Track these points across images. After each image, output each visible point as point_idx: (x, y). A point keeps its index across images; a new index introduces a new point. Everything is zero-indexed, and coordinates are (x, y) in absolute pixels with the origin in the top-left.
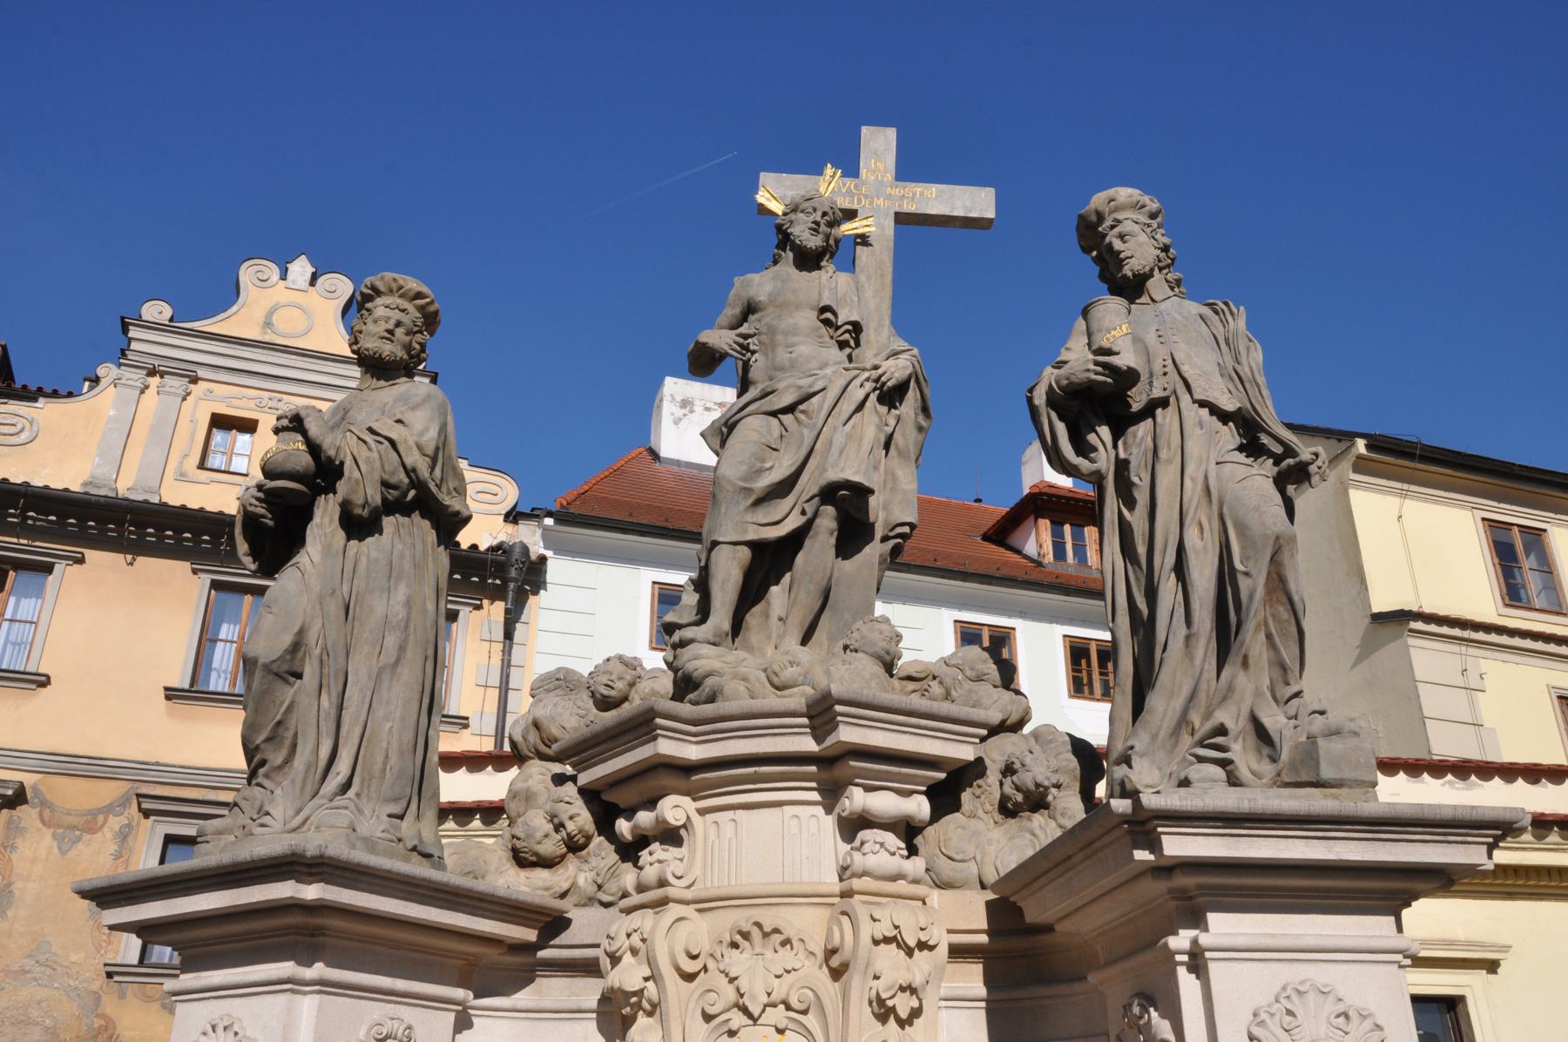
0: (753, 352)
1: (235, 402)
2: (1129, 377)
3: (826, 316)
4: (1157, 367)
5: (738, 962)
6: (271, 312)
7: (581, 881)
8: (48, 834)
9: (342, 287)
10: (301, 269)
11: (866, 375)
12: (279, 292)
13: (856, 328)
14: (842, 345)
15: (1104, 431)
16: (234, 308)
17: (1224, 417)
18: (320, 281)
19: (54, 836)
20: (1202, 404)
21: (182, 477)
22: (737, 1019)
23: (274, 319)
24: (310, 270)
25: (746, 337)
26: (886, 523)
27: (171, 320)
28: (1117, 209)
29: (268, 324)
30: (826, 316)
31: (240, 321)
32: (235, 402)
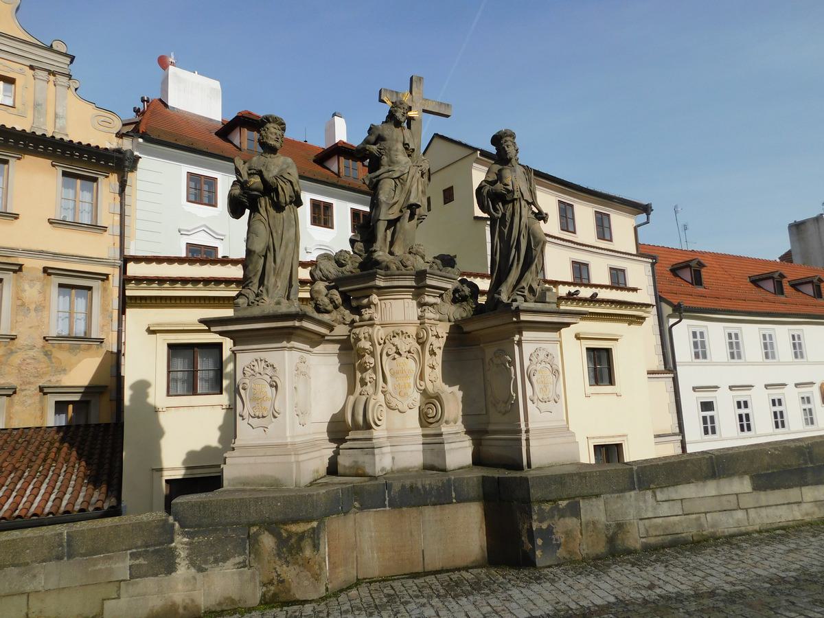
0: (383, 155)
2: (513, 192)
3: (406, 146)
4: (515, 188)
5: (396, 341)
7: (338, 317)
11: (419, 168)
13: (413, 150)
14: (409, 156)
15: (500, 204)
17: (529, 203)
20: (526, 200)
22: (397, 356)
25: (381, 149)
26: (419, 214)
28: (507, 136)
30: (406, 146)
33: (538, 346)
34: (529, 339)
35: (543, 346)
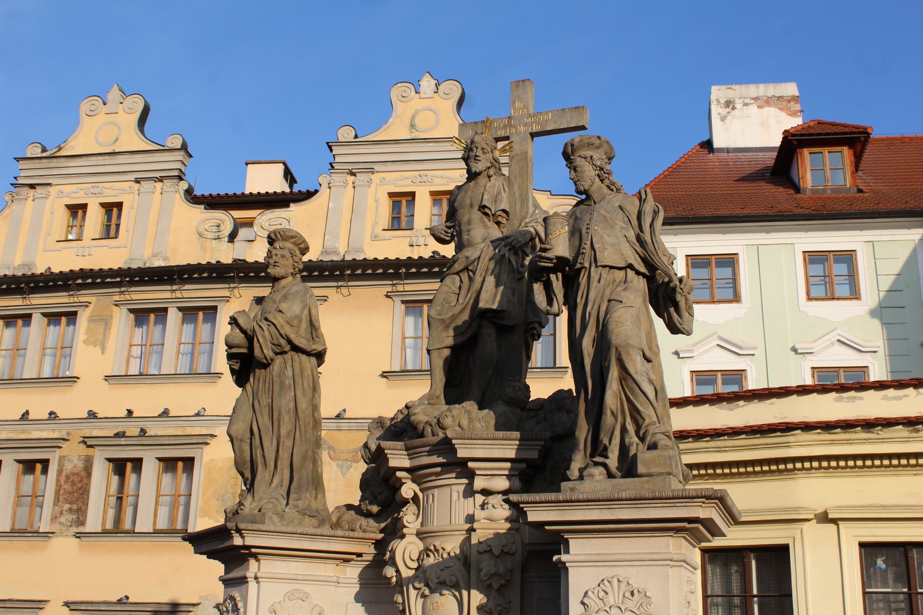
1: (399, 183)
6: (413, 118)
8: (334, 464)
9: (455, 91)
10: (427, 83)
12: (416, 103)
16: (391, 120)
18: (441, 88)
19: (338, 466)
21: (375, 238)
23: (416, 121)
24: (433, 82)
27: (356, 137)
29: (413, 126)
31: (396, 129)
32: (399, 183)
33: (606, 572)
34: (582, 558)
35: (622, 572)
